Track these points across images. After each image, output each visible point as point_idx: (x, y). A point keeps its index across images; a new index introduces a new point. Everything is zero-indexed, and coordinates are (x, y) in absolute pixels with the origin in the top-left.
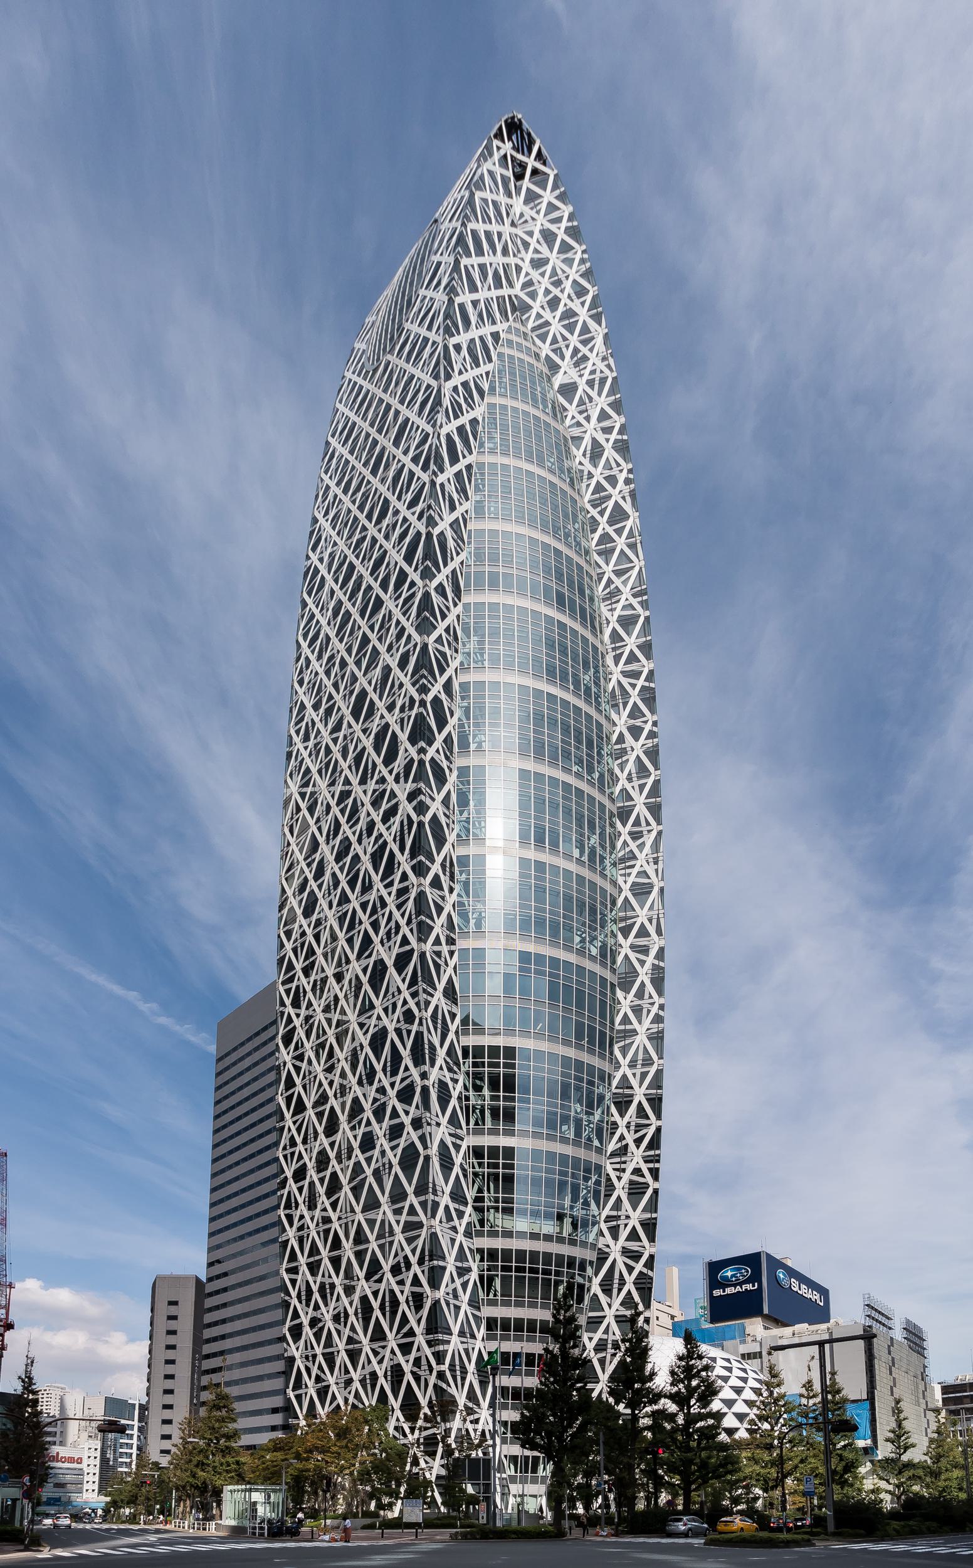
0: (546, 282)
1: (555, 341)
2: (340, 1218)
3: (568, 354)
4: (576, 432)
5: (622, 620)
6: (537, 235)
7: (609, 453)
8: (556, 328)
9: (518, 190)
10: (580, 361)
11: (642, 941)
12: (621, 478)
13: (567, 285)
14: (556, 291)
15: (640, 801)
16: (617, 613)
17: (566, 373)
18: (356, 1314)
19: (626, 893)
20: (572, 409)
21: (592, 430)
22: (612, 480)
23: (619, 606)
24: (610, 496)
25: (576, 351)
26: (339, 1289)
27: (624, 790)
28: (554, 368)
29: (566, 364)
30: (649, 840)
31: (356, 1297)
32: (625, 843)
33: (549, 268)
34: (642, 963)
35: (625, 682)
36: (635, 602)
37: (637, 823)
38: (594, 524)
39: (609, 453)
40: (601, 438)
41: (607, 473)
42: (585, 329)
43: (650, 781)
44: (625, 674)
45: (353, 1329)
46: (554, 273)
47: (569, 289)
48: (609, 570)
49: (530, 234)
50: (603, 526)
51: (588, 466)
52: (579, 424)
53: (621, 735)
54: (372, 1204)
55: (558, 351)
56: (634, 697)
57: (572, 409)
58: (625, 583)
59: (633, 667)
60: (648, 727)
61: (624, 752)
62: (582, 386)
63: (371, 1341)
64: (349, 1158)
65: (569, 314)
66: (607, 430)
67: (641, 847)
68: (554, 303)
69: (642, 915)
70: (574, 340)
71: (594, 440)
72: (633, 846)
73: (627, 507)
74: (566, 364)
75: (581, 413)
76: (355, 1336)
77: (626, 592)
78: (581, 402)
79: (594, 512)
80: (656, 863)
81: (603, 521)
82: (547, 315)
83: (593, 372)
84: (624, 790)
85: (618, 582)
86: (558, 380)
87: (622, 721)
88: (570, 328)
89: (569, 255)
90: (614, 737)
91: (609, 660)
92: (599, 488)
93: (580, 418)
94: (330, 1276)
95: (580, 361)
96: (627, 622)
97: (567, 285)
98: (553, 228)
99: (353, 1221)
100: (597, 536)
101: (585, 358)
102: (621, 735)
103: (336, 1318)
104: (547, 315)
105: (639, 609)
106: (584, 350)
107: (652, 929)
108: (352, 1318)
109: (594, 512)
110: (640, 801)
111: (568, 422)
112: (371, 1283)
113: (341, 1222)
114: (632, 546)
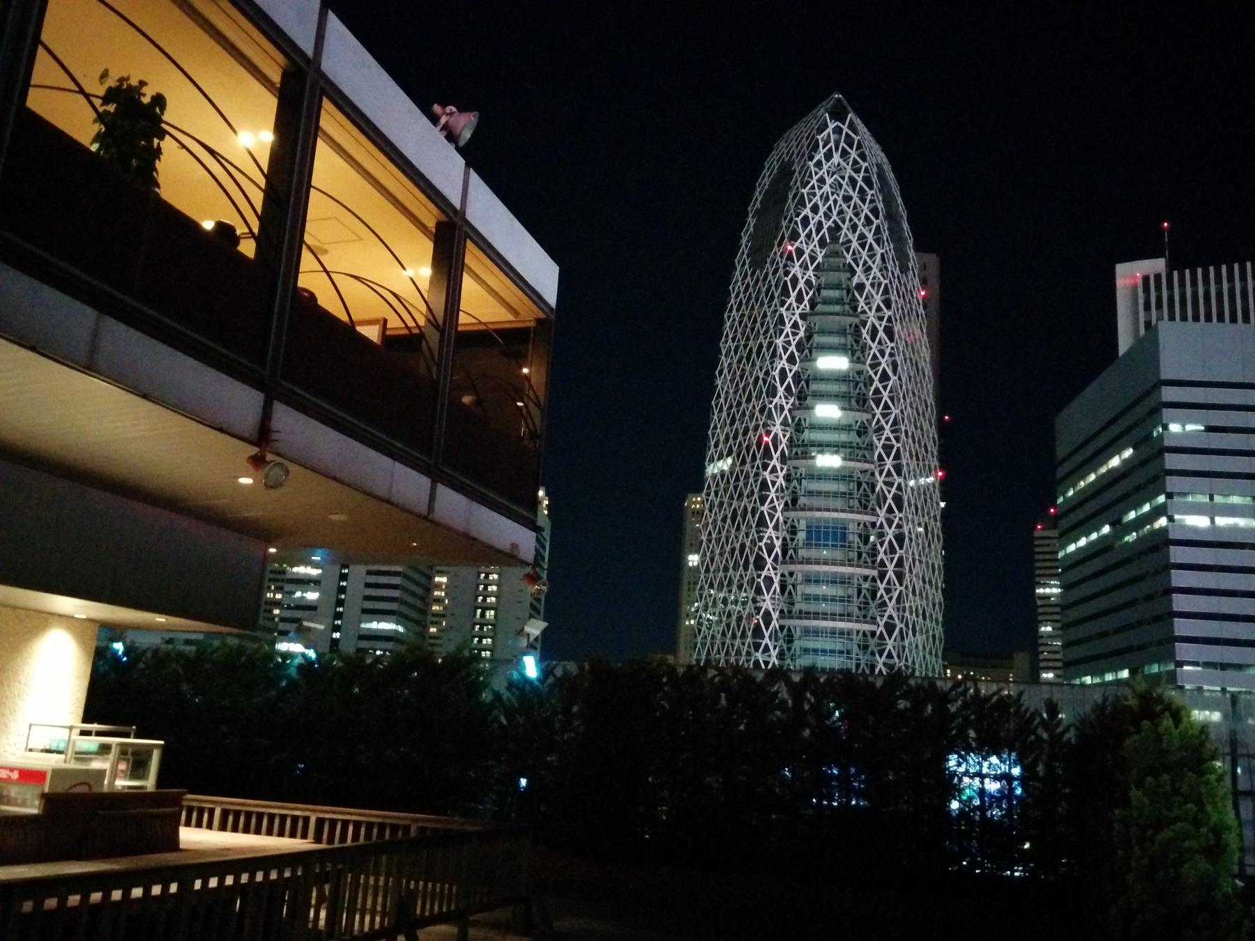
0: (849, 213)
1: (854, 253)
3: (861, 263)
4: (863, 317)
5: (884, 447)
7: (881, 334)
8: (855, 244)
9: (837, 149)
10: (868, 270)
12: (888, 351)
13: (863, 216)
15: (891, 568)
16: (882, 441)
19: (882, 628)
21: (872, 318)
22: (882, 353)
23: (884, 437)
24: (880, 364)
25: (865, 263)
27: (882, 560)
28: (853, 273)
29: (859, 270)
30: (896, 595)
32: (882, 596)
35: (884, 488)
36: (891, 436)
37: (889, 583)
38: (872, 381)
39: (881, 334)
42: (871, 248)
43: (897, 557)
44: (885, 483)
46: (855, 207)
48: (878, 412)
49: (843, 178)
50: (876, 383)
51: (869, 342)
52: (864, 312)
55: (855, 260)
56: (890, 501)
58: (887, 423)
59: (890, 479)
60: (896, 520)
61: (881, 535)
62: (868, 287)
65: (862, 237)
66: (881, 319)
67: (890, 599)
68: (854, 228)
69: (890, 644)
70: (864, 254)
71: (873, 325)
72: (886, 598)
73: (890, 373)
74: (859, 270)
77: (887, 427)
78: (867, 298)
79: (871, 373)
81: (876, 378)
84: (882, 560)
85: (883, 422)
86: (855, 280)
87: (882, 513)
88: (863, 246)
92: (875, 357)
93: (866, 308)
95: (868, 270)
96: (888, 448)
97: (863, 216)
98: (855, 176)
100: (873, 388)
101: (869, 269)
104: (850, 236)
105: (894, 442)
106: (870, 263)
107: (895, 655)
109: (871, 373)
110: (891, 568)
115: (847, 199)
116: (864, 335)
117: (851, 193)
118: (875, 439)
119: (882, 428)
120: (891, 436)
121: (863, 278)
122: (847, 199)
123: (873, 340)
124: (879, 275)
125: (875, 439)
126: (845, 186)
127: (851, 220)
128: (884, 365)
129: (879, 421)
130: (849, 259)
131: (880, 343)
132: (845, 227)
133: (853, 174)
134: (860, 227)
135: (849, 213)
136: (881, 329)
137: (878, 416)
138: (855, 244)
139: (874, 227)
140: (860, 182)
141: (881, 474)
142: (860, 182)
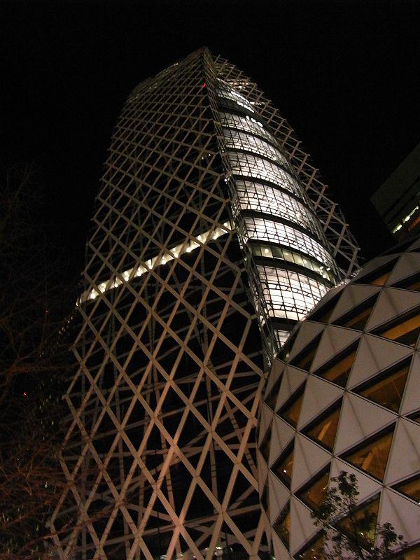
2: (143, 390)
11: (345, 247)
18: (164, 489)
26: (138, 461)
31: (164, 469)
34: (351, 257)
45: (159, 507)
54: (188, 368)
63: (187, 518)
64: (158, 336)
67: (329, 210)
76: (162, 516)
80: (340, 216)
94: (126, 448)
99: (161, 391)
103: (132, 498)
108: (157, 493)
112: (187, 449)
113: (144, 393)
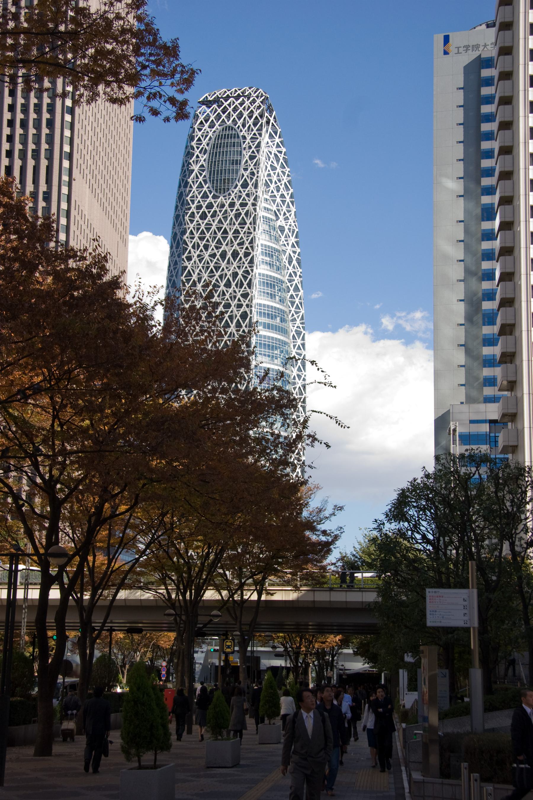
0: (275, 178)
4: (284, 248)
5: (296, 331)
6: (273, 155)
7: (294, 262)
10: (287, 219)
12: (298, 274)
13: (283, 183)
14: (279, 184)
16: (295, 328)
17: (281, 222)
20: (283, 238)
23: (296, 325)
25: (285, 214)
29: (281, 217)
33: (277, 172)
36: (301, 326)
39: (294, 262)
40: (292, 255)
41: (294, 270)
42: (288, 206)
46: (278, 175)
47: (283, 185)
49: (271, 153)
51: (287, 265)
53: (294, 377)
57: (283, 238)
58: (298, 317)
61: (294, 383)
62: (286, 230)
65: (282, 196)
66: (294, 252)
74: (281, 217)
75: (286, 241)
78: (286, 237)
79: (289, 284)
81: (292, 289)
82: (275, 193)
83: (290, 225)
86: (279, 223)
89: (284, 170)
90: (292, 377)
91: (292, 347)
93: (285, 243)
95: (287, 219)
97: (283, 183)
98: (279, 155)
100: (290, 294)
102: (294, 377)
104: (275, 193)
105: (302, 330)
111: (281, 243)
114: (301, 303)
115: (274, 168)
116: (284, 260)
117: (275, 165)
118: (291, 325)
119: (294, 320)
120: (301, 326)
121: (283, 222)
122: (274, 168)
123: (290, 265)
124: (293, 224)
125: (291, 325)
126: (271, 159)
127: (276, 183)
128: (296, 281)
129: (293, 315)
130: (274, 208)
131: (294, 267)
132: (272, 186)
133: (277, 153)
134: (281, 190)
135: (275, 178)
136: (294, 259)
137: (293, 312)
138: (278, 200)
139: (290, 192)
140: (281, 160)
141: (294, 346)
142: (281, 160)
